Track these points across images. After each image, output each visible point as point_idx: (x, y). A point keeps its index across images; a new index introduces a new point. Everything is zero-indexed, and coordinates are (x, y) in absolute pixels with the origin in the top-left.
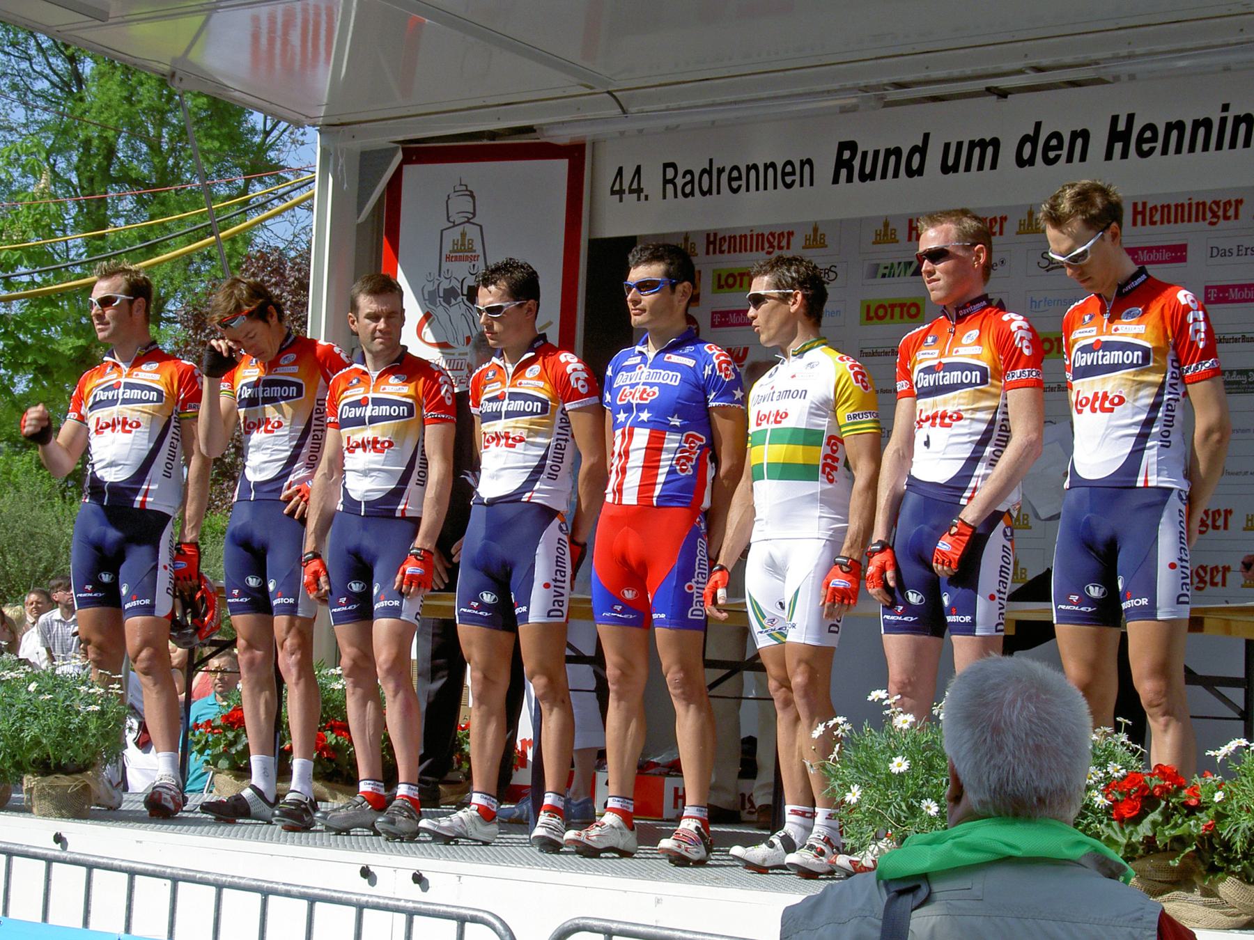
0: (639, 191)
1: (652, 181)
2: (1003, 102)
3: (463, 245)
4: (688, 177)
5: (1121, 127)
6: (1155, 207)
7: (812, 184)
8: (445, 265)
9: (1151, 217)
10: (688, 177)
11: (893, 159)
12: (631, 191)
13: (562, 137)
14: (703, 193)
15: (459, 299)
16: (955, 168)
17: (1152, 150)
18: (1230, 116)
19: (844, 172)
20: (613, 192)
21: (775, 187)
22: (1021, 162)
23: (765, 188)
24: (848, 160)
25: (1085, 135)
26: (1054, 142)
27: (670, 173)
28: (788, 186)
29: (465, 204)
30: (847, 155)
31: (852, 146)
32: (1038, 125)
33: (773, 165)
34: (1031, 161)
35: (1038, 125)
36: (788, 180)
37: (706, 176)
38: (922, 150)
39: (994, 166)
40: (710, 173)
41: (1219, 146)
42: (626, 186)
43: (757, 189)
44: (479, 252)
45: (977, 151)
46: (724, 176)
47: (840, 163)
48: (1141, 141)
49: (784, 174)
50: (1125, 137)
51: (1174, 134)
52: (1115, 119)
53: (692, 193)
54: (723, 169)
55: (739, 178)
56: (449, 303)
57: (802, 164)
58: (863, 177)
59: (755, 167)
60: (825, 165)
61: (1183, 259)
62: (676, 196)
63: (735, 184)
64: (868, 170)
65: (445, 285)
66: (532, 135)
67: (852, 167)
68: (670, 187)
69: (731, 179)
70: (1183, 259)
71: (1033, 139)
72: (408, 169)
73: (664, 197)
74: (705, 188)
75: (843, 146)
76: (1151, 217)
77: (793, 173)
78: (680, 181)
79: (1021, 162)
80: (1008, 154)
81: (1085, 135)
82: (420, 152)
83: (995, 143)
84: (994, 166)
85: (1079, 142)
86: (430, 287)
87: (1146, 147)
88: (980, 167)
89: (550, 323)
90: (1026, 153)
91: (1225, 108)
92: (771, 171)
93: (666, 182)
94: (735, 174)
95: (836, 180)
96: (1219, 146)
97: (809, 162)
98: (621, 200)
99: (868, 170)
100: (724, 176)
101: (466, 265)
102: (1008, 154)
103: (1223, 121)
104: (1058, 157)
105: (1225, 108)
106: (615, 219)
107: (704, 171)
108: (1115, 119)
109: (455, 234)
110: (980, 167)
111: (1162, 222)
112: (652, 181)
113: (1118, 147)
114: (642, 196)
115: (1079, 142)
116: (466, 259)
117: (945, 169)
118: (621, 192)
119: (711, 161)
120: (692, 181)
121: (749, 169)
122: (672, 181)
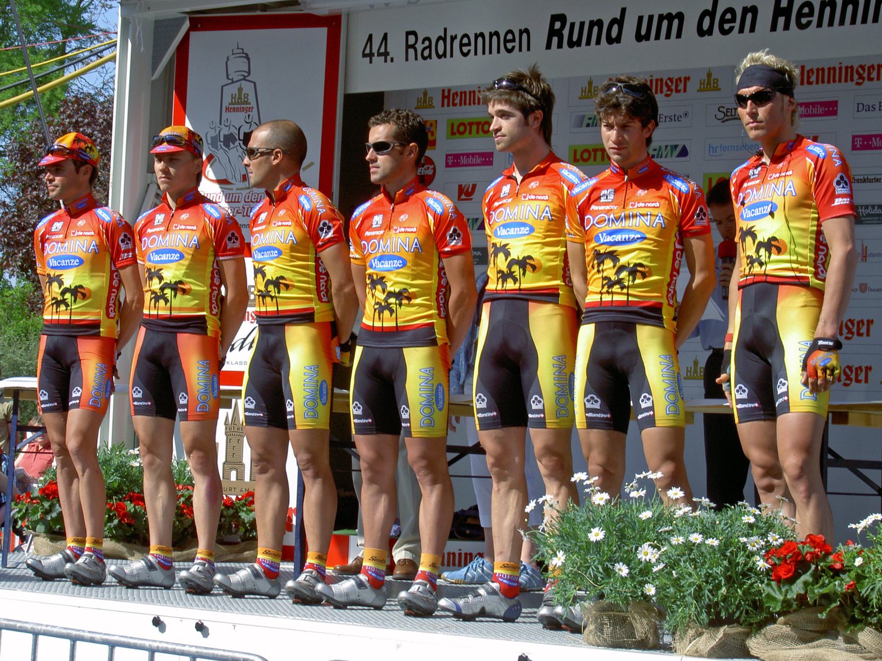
0: (386, 54)
1: (396, 46)
3: (240, 98)
4: (427, 43)
6: (812, 70)
7: (529, 49)
8: (226, 115)
9: (809, 78)
10: (427, 43)
11: (595, 29)
12: (379, 54)
13: (322, 8)
14: (439, 57)
15: (237, 143)
16: (647, 37)
17: (809, 23)
19: (555, 40)
20: (364, 55)
21: (499, 52)
22: (701, 32)
23: (490, 52)
24: (558, 30)
25: (754, 10)
26: (728, 16)
27: (412, 39)
28: (509, 51)
29: (242, 65)
30: (558, 25)
31: (562, 18)
33: (497, 34)
34: (710, 32)
37: (441, 43)
38: (619, 22)
39: (679, 35)
42: (375, 51)
43: (484, 53)
44: (253, 104)
45: (665, 23)
46: (456, 43)
47: (552, 32)
48: (800, 15)
49: (506, 41)
50: (787, 12)
53: (430, 56)
54: (456, 37)
56: (228, 146)
58: (571, 44)
60: (540, 35)
61: (834, 113)
62: (416, 59)
64: (575, 38)
65: (225, 131)
66: (298, 7)
67: (562, 35)
68: (411, 51)
69: (462, 45)
70: (834, 113)
71: (711, 14)
72: (193, 34)
73: (407, 59)
74: (441, 52)
75: (554, 18)
76: (809, 78)
77: (513, 40)
78: (420, 46)
79: (701, 32)
80: (690, 25)
81: (754, 10)
83: (680, 16)
84: (679, 35)
85: (749, 16)
87: (804, 21)
88: (668, 36)
89: (312, 164)
92: (495, 38)
93: (408, 47)
94: (465, 41)
95: (548, 47)
97: (527, 31)
98: (371, 62)
99: (575, 38)
100: (456, 43)
101: (242, 115)
102: (690, 25)
104: (732, 28)
106: (364, 78)
107: (440, 38)
109: (233, 89)
110: (668, 36)
111: (817, 83)
112: (396, 46)
113: (781, 20)
114: (389, 58)
115: (749, 16)
116: (243, 110)
117: (639, 38)
118: (371, 55)
119: (445, 30)
120: (430, 47)
121: (476, 36)
122: (413, 46)
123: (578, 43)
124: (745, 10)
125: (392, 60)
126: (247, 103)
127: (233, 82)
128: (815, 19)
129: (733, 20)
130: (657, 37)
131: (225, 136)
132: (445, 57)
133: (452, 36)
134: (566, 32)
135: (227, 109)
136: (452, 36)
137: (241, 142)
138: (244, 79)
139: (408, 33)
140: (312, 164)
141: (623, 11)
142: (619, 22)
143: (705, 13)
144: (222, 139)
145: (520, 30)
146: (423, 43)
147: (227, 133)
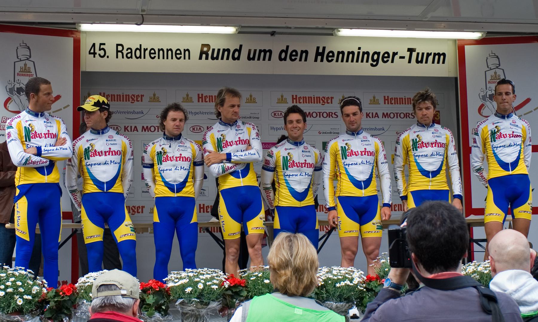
2: (273, 37)
3: (25, 69)
4: (129, 51)
5: (321, 50)
7: (189, 58)
10: (129, 51)
14: (137, 58)
16: (253, 59)
19: (204, 56)
20: (90, 53)
21: (172, 58)
22: (281, 59)
23: (167, 58)
25: (306, 52)
31: (208, 46)
32: (288, 47)
34: (285, 59)
35: (288, 47)
36: (178, 56)
38: (239, 51)
39: (269, 59)
41: (357, 61)
43: (163, 58)
45: (262, 54)
46: (147, 52)
48: (328, 56)
49: (176, 54)
50: (322, 54)
52: (318, 48)
53: (131, 57)
54: (147, 49)
55: (155, 53)
56: (20, 94)
57: (185, 51)
58: (213, 58)
59: (162, 50)
60: (195, 53)
63: (153, 56)
64: (215, 56)
65: (17, 86)
68: (120, 54)
69: (150, 53)
73: (117, 57)
75: (203, 46)
78: (125, 52)
79: (281, 59)
81: (306, 52)
83: (270, 51)
84: (269, 59)
85: (304, 54)
86: (10, 86)
88: (264, 59)
89: (68, 106)
90: (283, 55)
91: (359, 48)
92: (170, 52)
93: (118, 51)
94: (152, 51)
95: (200, 58)
96: (357, 61)
97: (188, 50)
99: (215, 56)
100: (147, 52)
103: (359, 53)
105: (359, 48)
107: (137, 49)
108: (318, 48)
109: (22, 64)
113: (319, 58)
115: (304, 54)
117: (249, 58)
119: (141, 45)
120: (131, 52)
121: (159, 50)
123: (217, 58)
124: (302, 52)
125: (108, 57)
127: (21, 61)
130: (259, 59)
131: (17, 88)
132: (141, 58)
134: (210, 53)
135: (18, 74)
138: (28, 59)
139: (118, 45)
140: (68, 106)
141: (241, 46)
144: (16, 90)
145: (184, 50)
146: (127, 50)
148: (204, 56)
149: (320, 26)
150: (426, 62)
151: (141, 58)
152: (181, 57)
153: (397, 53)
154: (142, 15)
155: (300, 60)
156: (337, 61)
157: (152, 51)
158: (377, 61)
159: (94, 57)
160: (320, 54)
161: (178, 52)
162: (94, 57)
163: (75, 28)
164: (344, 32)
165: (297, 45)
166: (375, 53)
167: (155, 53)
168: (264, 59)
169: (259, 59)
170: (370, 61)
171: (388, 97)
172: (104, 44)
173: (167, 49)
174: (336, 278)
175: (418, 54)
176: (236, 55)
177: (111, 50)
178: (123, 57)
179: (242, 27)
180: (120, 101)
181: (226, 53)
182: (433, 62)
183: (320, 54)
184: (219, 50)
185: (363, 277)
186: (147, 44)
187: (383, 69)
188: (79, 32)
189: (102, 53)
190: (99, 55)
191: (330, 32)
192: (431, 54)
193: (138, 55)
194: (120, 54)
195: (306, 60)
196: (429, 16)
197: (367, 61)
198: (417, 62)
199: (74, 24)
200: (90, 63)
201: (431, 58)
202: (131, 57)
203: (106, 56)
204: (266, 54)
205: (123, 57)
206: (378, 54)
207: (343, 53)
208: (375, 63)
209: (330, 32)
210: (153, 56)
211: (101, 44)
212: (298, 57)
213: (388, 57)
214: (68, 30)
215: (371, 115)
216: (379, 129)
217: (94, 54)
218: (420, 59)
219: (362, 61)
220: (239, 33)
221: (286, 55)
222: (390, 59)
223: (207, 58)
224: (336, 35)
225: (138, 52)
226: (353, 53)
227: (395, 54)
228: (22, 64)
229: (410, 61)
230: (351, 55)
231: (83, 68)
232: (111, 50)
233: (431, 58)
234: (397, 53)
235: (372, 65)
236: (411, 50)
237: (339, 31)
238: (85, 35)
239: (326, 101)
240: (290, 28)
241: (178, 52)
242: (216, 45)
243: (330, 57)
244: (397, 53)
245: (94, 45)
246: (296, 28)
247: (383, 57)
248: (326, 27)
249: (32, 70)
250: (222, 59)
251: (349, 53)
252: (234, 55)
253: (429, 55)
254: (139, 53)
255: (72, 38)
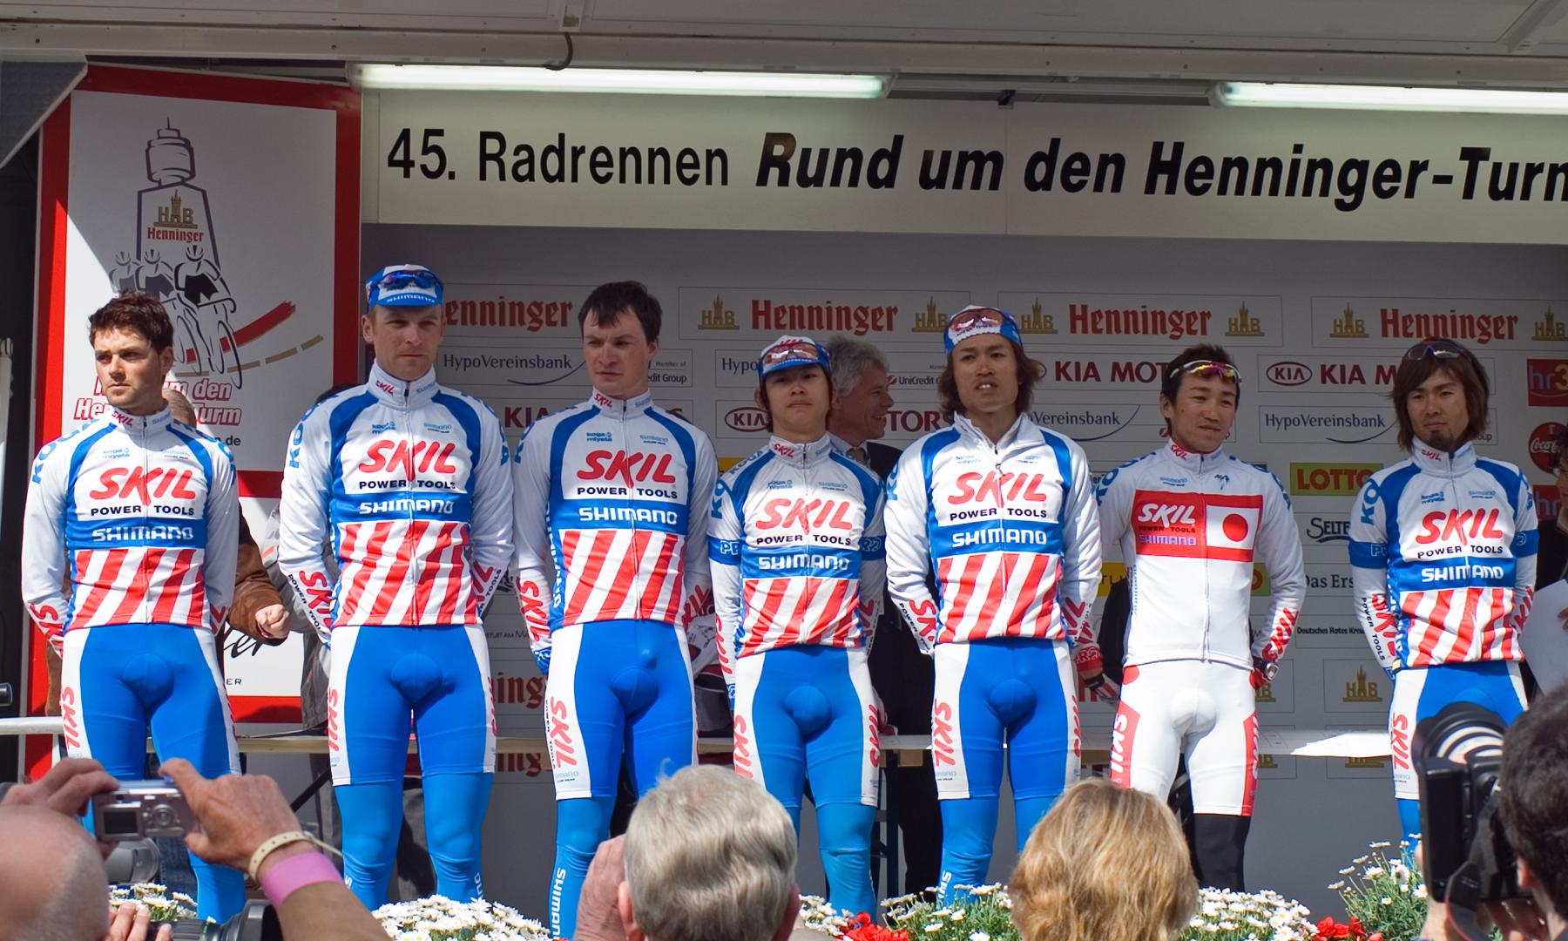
2: (1004, 112)
3: (175, 216)
4: (524, 155)
5: (1167, 155)
7: (725, 182)
10: (524, 155)
14: (549, 179)
15: (173, 294)
16: (940, 183)
18: (1304, 158)
19: (774, 173)
20: (392, 163)
21: (667, 181)
22: (1032, 184)
23: (651, 180)
25: (1119, 161)
26: (1077, 165)
31: (787, 139)
32: (1055, 143)
34: (1046, 185)
35: (1055, 143)
36: (688, 173)
38: (892, 155)
39: (994, 185)
40: (560, 153)
41: (1291, 191)
43: (638, 180)
44: (203, 227)
45: (971, 166)
46: (584, 160)
47: (768, 161)
48: (1191, 174)
50: (1172, 168)
51: (1235, 172)
52: (1158, 147)
53: (530, 176)
54: (583, 150)
55: (609, 163)
57: (710, 155)
58: (804, 181)
59: (634, 151)
60: (745, 162)
63: (602, 172)
65: (148, 272)
68: (492, 166)
69: (594, 164)
73: (483, 177)
75: (772, 139)
78: (509, 159)
79: (1032, 184)
80: (1014, 172)
81: (1119, 161)
82: (108, 76)
83: (997, 158)
84: (994, 185)
85: (1111, 169)
86: (123, 273)
88: (976, 185)
89: (319, 339)
90: (1040, 171)
91: (1298, 149)
92: (659, 160)
93: (485, 157)
94: (602, 157)
95: (762, 180)
96: (1291, 191)
97: (721, 153)
100: (584, 160)
102: (1014, 172)
103: (1295, 164)
105: (1298, 149)
108: (1158, 147)
109: (164, 198)
113: (1162, 180)
115: (1111, 169)
116: (183, 236)
117: (926, 182)
119: (562, 137)
120: (530, 161)
122: (496, 157)
123: (818, 181)
125: (452, 175)
126: (190, 224)
127: (161, 187)
128: (1215, 182)
129: (1085, 171)
132: (562, 180)
133: (574, 149)
134: (794, 163)
135: (151, 233)
136: (574, 149)
137: (182, 294)
138: (183, 182)
139: (485, 136)
140: (319, 339)
141: (898, 140)
142: (892, 155)
143: (1037, 158)
146: (516, 153)
147: (152, 275)
148: (774, 173)
149: (1166, 75)
150: (1526, 195)
151: (562, 180)
152: (696, 177)
153: (1424, 166)
154: (567, 35)
155: (1099, 187)
156: (1222, 190)
157: (602, 157)
158: (1359, 190)
159: (407, 175)
160: (1163, 167)
161: (688, 159)
162: (407, 175)
163: (344, 80)
164: (1248, 94)
165: (1087, 137)
166: (1350, 164)
167: (609, 163)
168: (976, 185)
169: (958, 184)
170: (1334, 191)
171: (1395, 312)
172: (440, 133)
173: (651, 150)
174: (1213, 928)
175: (1497, 167)
176: (883, 168)
177: (462, 150)
178: (502, 177)
179: (903, 76)
180: (492, 323)
181: (848, 163)
182: (1549, 195)
183: (1163, 167)
184: (824, 153)
185: (1308, 925)
186: (585, 134)
187: (1379, 219)
188: (356, 91)
189: (432, 162)
190: (424, 168)
191: (1198, 92)
192: (1540, 168)
193: (553, 169)
194: (492, 166)
195: (1116, 188)
196: (1535, 40)
197: (1325, 192)
198: (1495, 194)
199: (340, 64)
200: (393, 199)
201: (1540, 181)
202: (530, 176)
203: (446, 174)
204: (983, 166)
205: (502, 177)
206: (1362, 166)
207: (1242, 163)
208: (1349, 199)
209: (1202, 94)
210: (602, 172)
211: (429, 133)
212: (1091, 179)
213: (1393, 178)
214: (323, 87)
215: (1336, 374)
216: (1367, 422)
217: (407, 164)
218: (1502, 186)
219: (1307, 192)
220: (893, 95)
221: (1054, 170)
222: (1403, 185)
223: (783, 181)
224: (1220, 105)
225: (553, 159)
226: (1276, 164)
227: (1417, 168)
228: (164, 198)
229: (1468, 193)
230: (1269, 172)
231: (367, 214)
232: (462, 150)
233: (1540, 181)
234: (1426, 164)
235: (1340, 205)
236: (1473, 156)
237: (1230, 90)
238: (375, 101)
239: (1184, 325)
240: (1064, 79)
241: (688, 159)
242: (811, 136)
243: (1198, 178)
244: (1424, 166)
245: (405, 136)
246: (1083, 79)
247: (1379, 177)
248: (1185, 75)
249: (199, 219)
250: (836, 182)
251: (1262, 164)
252: (878, 169)
253: (1533, 170)
254: (557, 161)
255: (333, 114)
